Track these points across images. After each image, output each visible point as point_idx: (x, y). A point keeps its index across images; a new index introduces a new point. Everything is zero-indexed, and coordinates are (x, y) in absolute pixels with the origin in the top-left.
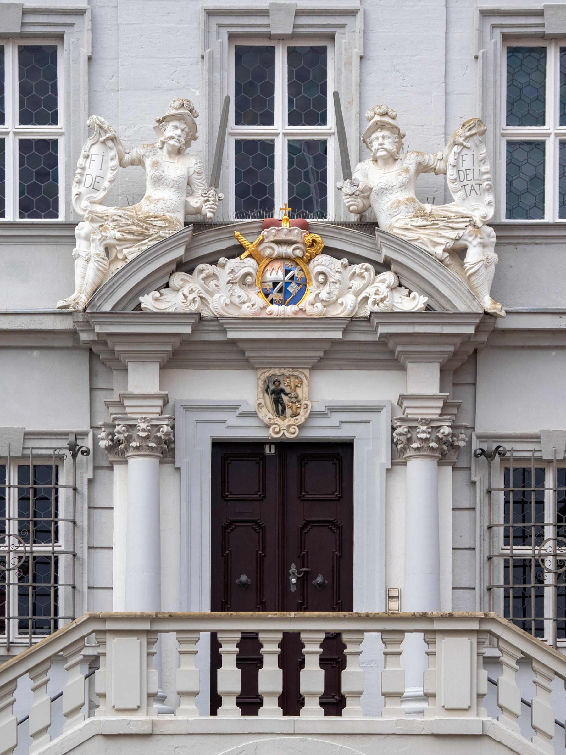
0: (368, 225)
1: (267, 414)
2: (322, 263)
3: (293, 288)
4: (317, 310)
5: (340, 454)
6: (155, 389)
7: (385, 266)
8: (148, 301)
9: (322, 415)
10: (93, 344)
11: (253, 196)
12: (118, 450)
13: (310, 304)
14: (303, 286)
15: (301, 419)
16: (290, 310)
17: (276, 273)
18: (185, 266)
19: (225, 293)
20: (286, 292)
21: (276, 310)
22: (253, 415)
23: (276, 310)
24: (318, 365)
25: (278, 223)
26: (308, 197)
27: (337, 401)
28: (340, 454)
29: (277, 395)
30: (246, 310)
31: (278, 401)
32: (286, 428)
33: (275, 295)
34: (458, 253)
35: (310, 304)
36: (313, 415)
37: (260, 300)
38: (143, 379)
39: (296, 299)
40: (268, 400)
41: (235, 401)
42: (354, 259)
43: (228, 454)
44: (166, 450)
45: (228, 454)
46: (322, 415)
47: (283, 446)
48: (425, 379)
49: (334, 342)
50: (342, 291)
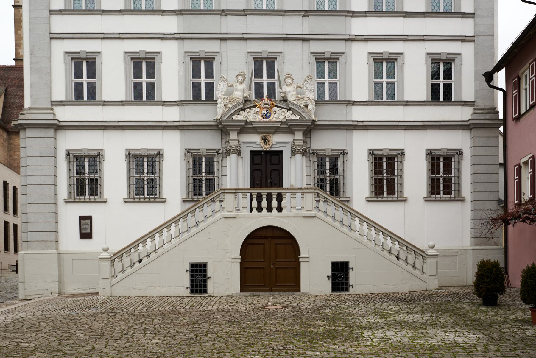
0: (285, 100)
1: (262, 144)
2: (275, 109)
3: (268, 115)
4: (274, 120)
5: (279, 154)
6: (236, 138)
7: (289, 109)
8: (234, 117)
9: (275, 145)
10: (222, 128)
11: (259, 94)
12: (228, 153)
13: (273, 118)
14: (271, 114)
15: (270, 145)
16: (267, 120)
17: (264, 111)
18: (243, 109)
19: (252, 116)
21: (264, 120)
22: (259, 144)
23: (264, 120)
24: (274, 133)
25: (265, 100)
27: (278, 141)
28: (279, 154)
29: (265, 140)
30: (258, 120)
31: (265, 141)
32: (267, 148)
33: (264, 116)
34: (307, 106)
35: (273, 118)
36: (273, 145)
37: (261, 118)
38: (234, 136)
39: (269, 117)
40: (263, 141)
41: (254, 141)
42: (282, 108)
43: (253, 153)
44: (239, 153)
45: (253, 153)
46: (275, 145)
47: (267, 152)
48: (299, 136)
49: (278, 127)
50: (280, 115)
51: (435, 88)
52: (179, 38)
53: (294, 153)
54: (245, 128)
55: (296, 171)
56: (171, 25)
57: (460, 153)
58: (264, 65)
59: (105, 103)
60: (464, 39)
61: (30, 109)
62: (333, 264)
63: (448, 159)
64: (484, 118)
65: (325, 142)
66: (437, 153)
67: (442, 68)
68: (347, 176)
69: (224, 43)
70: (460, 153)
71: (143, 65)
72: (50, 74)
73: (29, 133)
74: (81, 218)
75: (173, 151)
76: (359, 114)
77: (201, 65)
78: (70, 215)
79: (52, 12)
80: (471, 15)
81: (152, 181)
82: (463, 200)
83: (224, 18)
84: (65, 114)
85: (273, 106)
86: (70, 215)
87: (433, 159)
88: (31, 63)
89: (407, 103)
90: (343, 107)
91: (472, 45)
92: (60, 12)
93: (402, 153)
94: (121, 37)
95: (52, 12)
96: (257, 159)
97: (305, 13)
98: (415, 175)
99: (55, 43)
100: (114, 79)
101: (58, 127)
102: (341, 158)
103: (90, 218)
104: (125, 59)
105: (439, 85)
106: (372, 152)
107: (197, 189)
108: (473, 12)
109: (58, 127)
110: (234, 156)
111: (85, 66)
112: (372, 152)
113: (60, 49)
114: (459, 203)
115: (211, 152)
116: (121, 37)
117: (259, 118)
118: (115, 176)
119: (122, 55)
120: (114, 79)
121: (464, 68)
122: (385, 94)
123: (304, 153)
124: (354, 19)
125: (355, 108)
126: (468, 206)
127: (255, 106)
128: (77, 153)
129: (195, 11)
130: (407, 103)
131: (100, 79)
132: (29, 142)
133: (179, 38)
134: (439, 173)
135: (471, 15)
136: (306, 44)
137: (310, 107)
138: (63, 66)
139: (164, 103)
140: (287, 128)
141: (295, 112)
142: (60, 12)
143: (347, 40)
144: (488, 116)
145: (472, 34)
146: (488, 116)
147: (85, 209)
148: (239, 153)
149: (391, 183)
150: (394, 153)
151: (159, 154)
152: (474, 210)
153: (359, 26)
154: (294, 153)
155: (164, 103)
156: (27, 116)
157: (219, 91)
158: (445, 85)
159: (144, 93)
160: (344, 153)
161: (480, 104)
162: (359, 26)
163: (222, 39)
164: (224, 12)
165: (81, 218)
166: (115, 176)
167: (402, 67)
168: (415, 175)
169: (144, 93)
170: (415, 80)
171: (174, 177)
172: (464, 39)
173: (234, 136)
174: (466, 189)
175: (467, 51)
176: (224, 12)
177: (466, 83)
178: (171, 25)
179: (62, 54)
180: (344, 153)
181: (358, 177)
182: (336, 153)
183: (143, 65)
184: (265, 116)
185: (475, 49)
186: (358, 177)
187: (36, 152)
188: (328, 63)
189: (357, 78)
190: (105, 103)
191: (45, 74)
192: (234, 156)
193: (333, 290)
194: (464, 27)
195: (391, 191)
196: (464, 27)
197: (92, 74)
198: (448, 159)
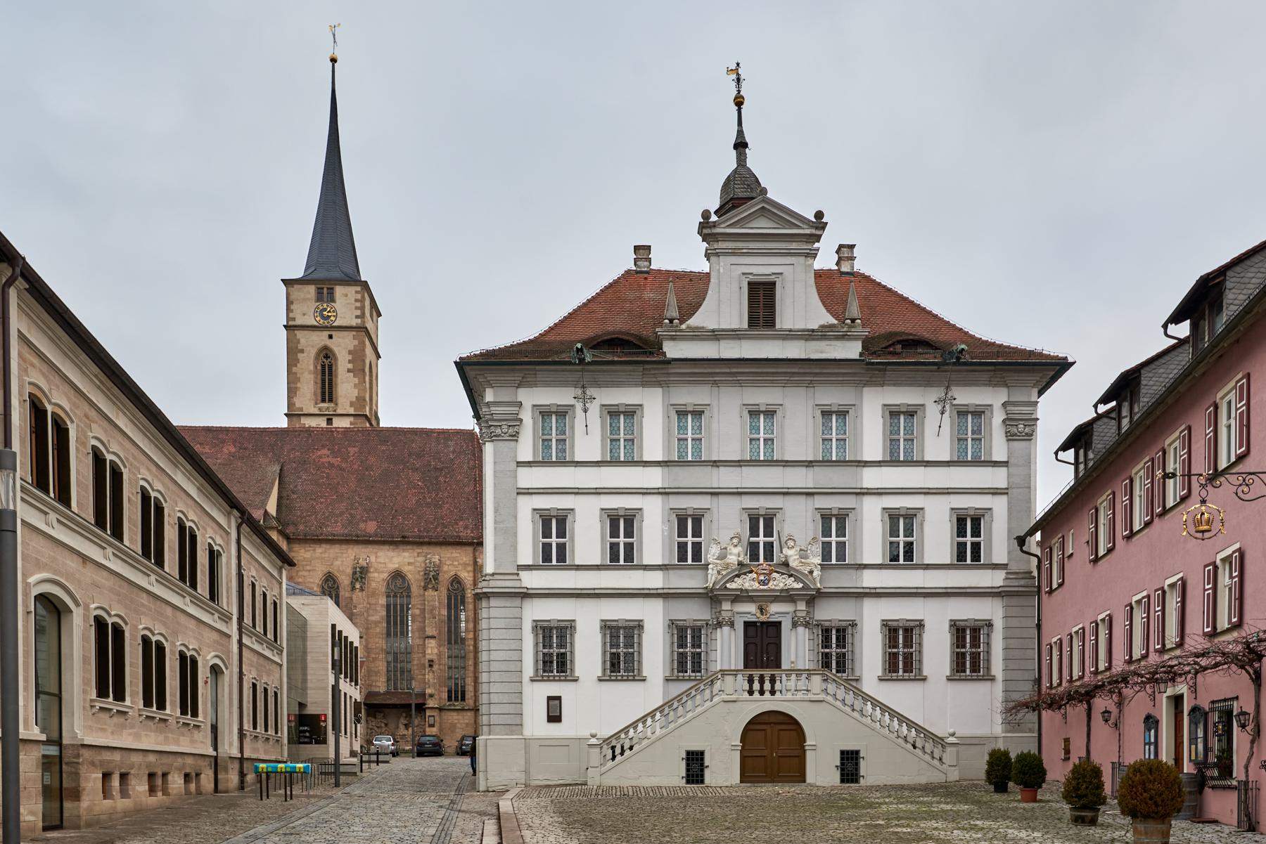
0: (786, 564)
2: (775, 575)
5: (778, 625)
7: (791, 576)
8: (728, 585)
10: (712, 597)
11: (754, 557)
12: (719, 625)
13: (771, 585)
17: (762, 578)
18: (738, 576)
19: (748, 583)
20: (763, 583)
26: (769, 555)
27: (777, 610)
28: (778, 625)
29: (761, 610)
32: (763, 618)
34: (811, 572)
35: (771, 585)
38: (726, 606)
41: (749, 610)
43: (747, 625)
44: (732, 625)
45: (747, 625)
47: (762, 623)
48: (802, 606)
50: (780, 582)
51: (961, 548)
52: (663, 492)
53: (795, 625)
54: (741, 597)
55: (798, 647)
56: (654, 478)
57: (989, 624)
58: (762, 522)
59: (579, 568)
60: (995, 492)
61: (493, 574)
62: (842, 752)
63: (976, 631)
64: (1016, 584)
65: (830, 613)
66: (962, 624)
67: (968, 524)
68: (857, 651)
69: (715, 499)
70: (989, 624)
71: (622, 524)
72: (515, 534)
73: (494, 602)
74: (549, 698)
75: (654, 621)
76: (870, 579)
77: (688, 524)
78: (536, 696)
79: (520, 464)
80: (1004, 464)
81: (629, 656)
82: (993, 679)
83: (715, 469)
84: (533, 580)
85: (771, 572)
86: (536, 696)
87: (958, 630)
88: (496, 522)
89: (928, 567)
90: (853, 572)
91: (1004, 499)
92: (529, 464)
93: (921, 624)
94: (597, 492)
95: (520, 464)
96: (752, 630)
97: (809, 464)
98: (936, 651)
99: (521, 499)
100: (588, 540)
101: (526, 595)
102: (850, 630)
103: (559, 698)
104: (601, 516)
105: (965, 544)
106: (885, 624)
107: (682, 667)
108: (1005, 459)
109: (526, 595)
110: (726, 629)
111: (554, 524)
112: (885, 624)
113: (526, 506)
114: (988, 684)
115: (699, 623)
116: (597, 492)
117: (756, 585)
118: (588, 652)
119: (598, 513)
120: (588, 540)
121: (995, 526)
122: (903, 554)
123: (807, 625)
124: (866, 469)
125: (867, 573)
126: (999, 687)
127: (751, 572)
128: (545, 624)
129: (682, 463)
130: (928, 567)
131: (572, 540)
132: (493, 613)
133: (663, 492)
134: (964, 647)
135: (1004, 464)
136: (810, 499)
137: (815, 574)
138: (531, 525)
139: (646, 568)
140: (787, 596)
141: (797, 579)
142: (529, 464)
143: (857, 494)
144: (1022, 582)
145: (1005, 486)
146: (1022, 582)
147: (553, 689)
148: (732, 625)
149: (908, 659)
150: (912, 624)
151: (639, 625)
152: (1005, 691)
153: (871, 478)
154: (795, 625)
155: (646, 568)
156: (492, 583)
157: (711, 553)
158: (972, 544)
159: (622, 554)
160: (854, 624)
161: (1014, 567)
162: (871, 478)
163: (712, 494)
164: (716, 464)
165: (549, 698)
166: (588, 652)
167: (922, 524)
168: (936, 651)
169: (622, 554)
170: (937, 540)
171: (655, 651)
172: (995, 492)
173: (726, 606)
174: (997, 667)
175: (999, 506)
176: (716, 464)
177: (998, 545)
178: (654, 478)
179: (529, 513)
180: (854, 624)
181: (870, 652)
182: (844, 624)
183: (622, 524)
184: (763, 583)
185: (1009, 503)
186: (870, 652)
187: (501, 623)
188: (835, 522)
189: (870, 540)
190: (579, 568)
191: (509, 534)
192: (726, 629)
193: (842, 781)
194: (998, 478)
195: (908, 668)
196: (998, 478)
197: (562, 533)
198: (976, 631)
